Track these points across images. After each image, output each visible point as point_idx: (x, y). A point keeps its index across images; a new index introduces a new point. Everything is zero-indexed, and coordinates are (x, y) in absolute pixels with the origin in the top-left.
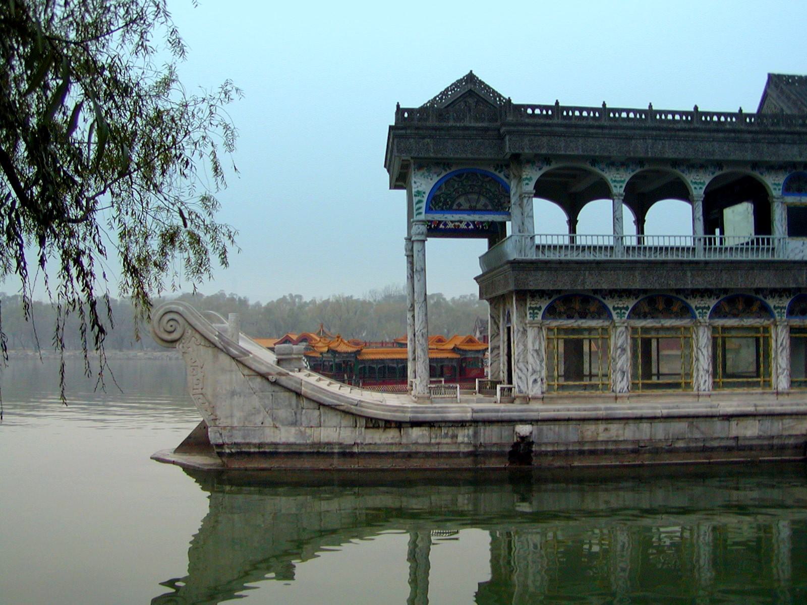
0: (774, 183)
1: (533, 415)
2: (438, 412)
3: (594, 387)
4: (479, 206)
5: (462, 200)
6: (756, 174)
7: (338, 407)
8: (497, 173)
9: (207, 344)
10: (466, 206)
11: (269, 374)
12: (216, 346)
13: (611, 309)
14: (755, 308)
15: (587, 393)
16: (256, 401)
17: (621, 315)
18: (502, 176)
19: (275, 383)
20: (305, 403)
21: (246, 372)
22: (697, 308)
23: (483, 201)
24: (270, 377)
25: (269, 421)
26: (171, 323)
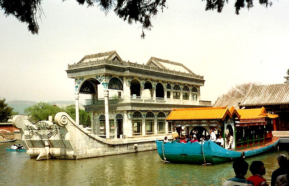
0: (165, 86)
1: (138, 142)
2: (121, 142)
3: (140, 135)
4: (117, 88)
5: (113, 86)
6: (162, 84)
7: (103, 142)
8: (119, 79)
9: (73, 125)
10: (114, 87)
11: (88, 133)
12: (75, 126)
13: (142, 115)
14: (163, 115)
15: (139, 136)
16: (84, 141)
17: (144, 116)
18: (120, 80)
19: (90, 136)
20: (95, 141)
21: (83, 133)
22: (155, 115)
23: (117, 86)
24: (88, 134)
25: (88, 147)
26: (64, 119)
